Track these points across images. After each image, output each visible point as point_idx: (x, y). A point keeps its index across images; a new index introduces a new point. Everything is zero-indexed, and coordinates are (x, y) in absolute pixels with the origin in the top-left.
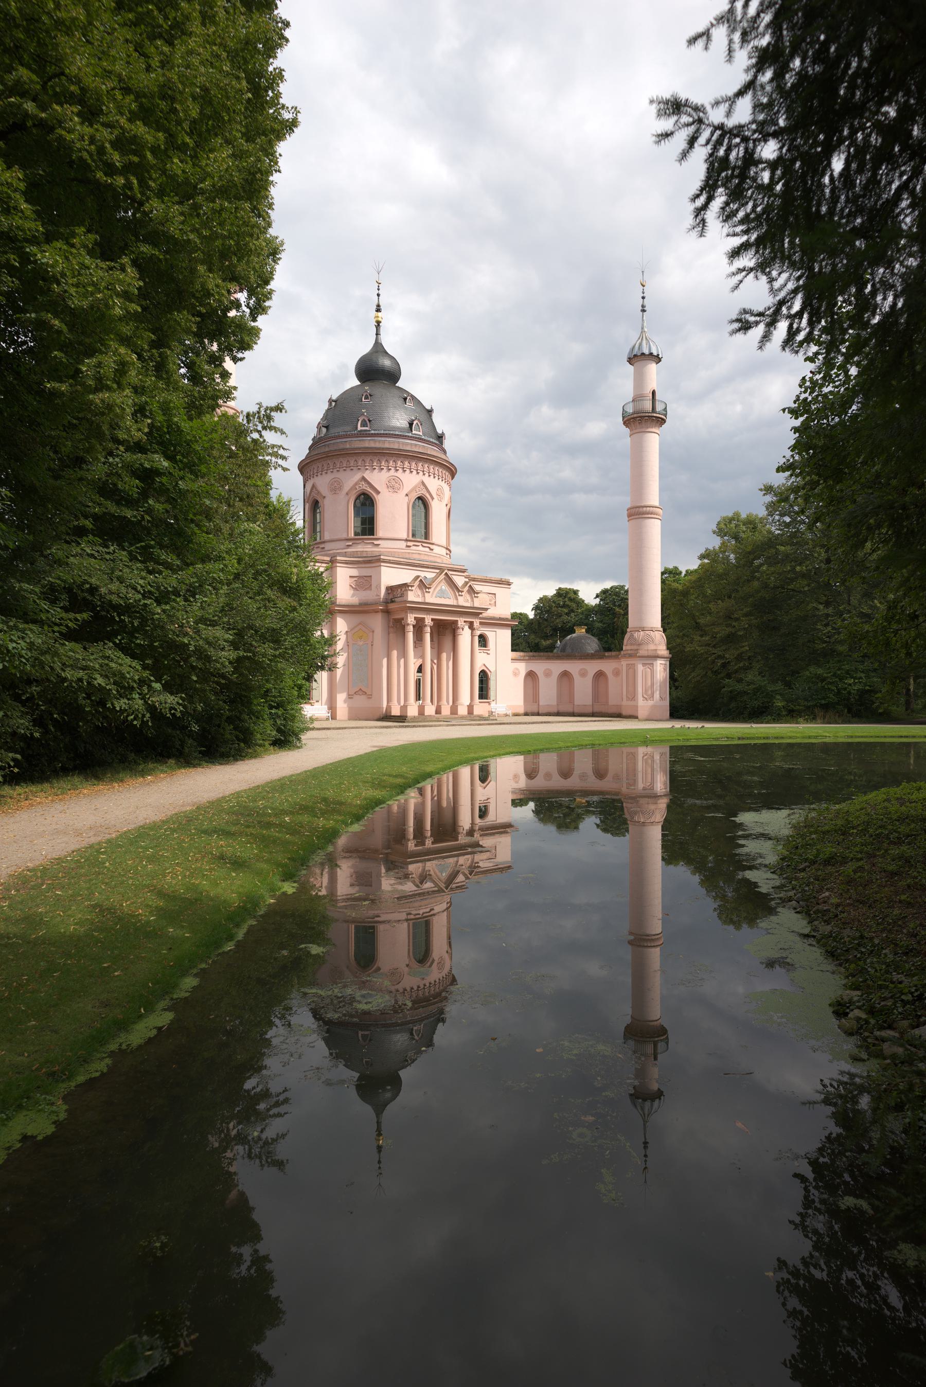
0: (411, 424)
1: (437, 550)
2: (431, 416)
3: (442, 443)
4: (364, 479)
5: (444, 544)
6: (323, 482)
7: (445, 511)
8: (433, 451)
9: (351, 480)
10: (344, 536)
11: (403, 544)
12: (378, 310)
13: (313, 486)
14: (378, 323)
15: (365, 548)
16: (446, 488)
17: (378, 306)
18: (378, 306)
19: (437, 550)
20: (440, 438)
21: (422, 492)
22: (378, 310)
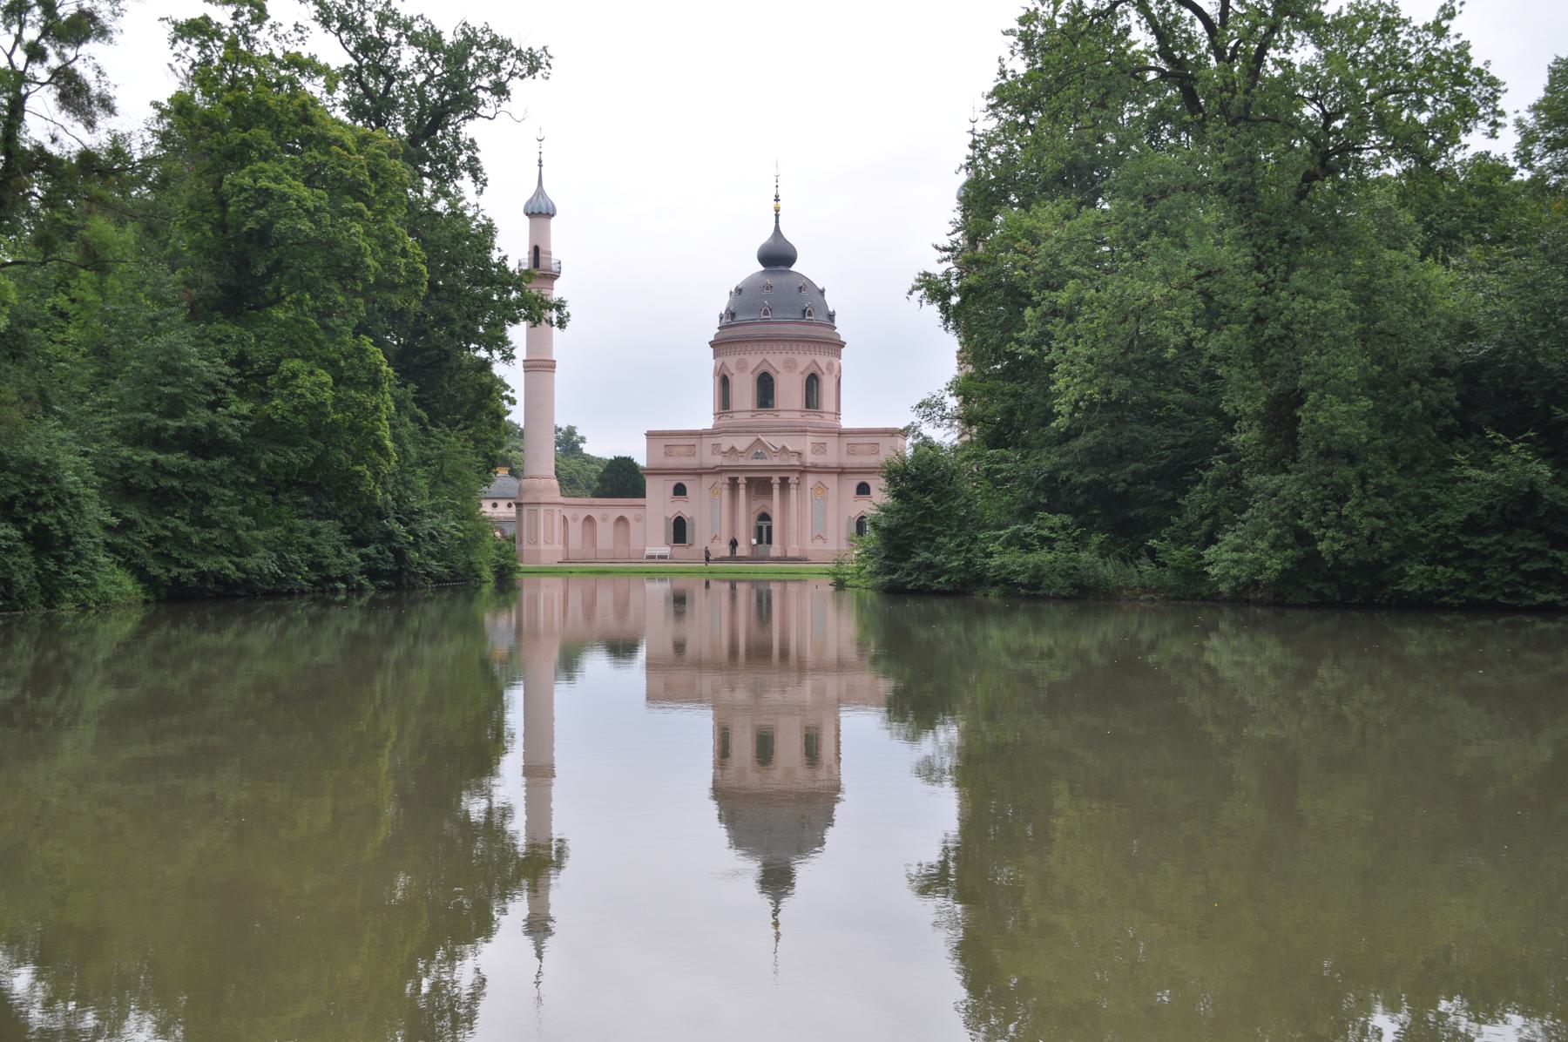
0: (805, 311)
1: (826, 416)
2: (823, 296)
3: (833, 321)
4: (765, 360)
5: (834, 410)
6: (731, 361)
7: (834, 382)
8: (823, 332)
9: (754, 360)
10: (750, 408)
11: (798, 415)
12: (777, 200)
13: (723, 364)
14: (777, 210)
15: (766, 417)
16: (834, 360)
17: (777, 196)
18: (777, 196)
19: (826, 416)
20: (831, 316)
21: (813, 369)
22: (777, 200)
